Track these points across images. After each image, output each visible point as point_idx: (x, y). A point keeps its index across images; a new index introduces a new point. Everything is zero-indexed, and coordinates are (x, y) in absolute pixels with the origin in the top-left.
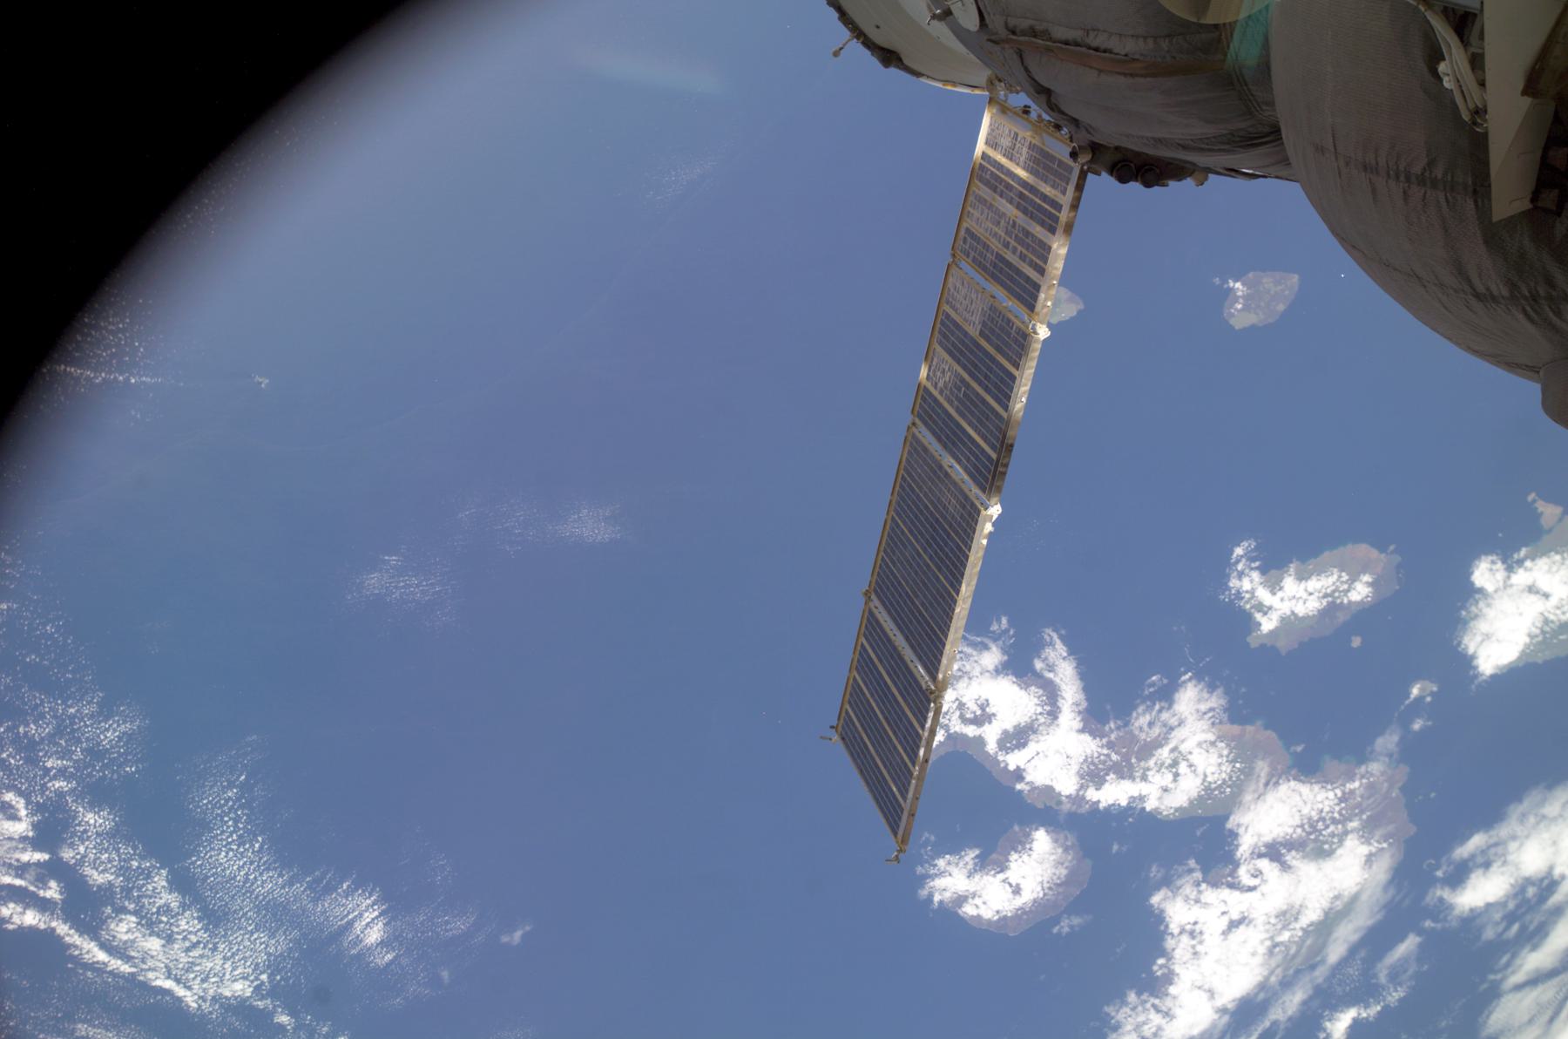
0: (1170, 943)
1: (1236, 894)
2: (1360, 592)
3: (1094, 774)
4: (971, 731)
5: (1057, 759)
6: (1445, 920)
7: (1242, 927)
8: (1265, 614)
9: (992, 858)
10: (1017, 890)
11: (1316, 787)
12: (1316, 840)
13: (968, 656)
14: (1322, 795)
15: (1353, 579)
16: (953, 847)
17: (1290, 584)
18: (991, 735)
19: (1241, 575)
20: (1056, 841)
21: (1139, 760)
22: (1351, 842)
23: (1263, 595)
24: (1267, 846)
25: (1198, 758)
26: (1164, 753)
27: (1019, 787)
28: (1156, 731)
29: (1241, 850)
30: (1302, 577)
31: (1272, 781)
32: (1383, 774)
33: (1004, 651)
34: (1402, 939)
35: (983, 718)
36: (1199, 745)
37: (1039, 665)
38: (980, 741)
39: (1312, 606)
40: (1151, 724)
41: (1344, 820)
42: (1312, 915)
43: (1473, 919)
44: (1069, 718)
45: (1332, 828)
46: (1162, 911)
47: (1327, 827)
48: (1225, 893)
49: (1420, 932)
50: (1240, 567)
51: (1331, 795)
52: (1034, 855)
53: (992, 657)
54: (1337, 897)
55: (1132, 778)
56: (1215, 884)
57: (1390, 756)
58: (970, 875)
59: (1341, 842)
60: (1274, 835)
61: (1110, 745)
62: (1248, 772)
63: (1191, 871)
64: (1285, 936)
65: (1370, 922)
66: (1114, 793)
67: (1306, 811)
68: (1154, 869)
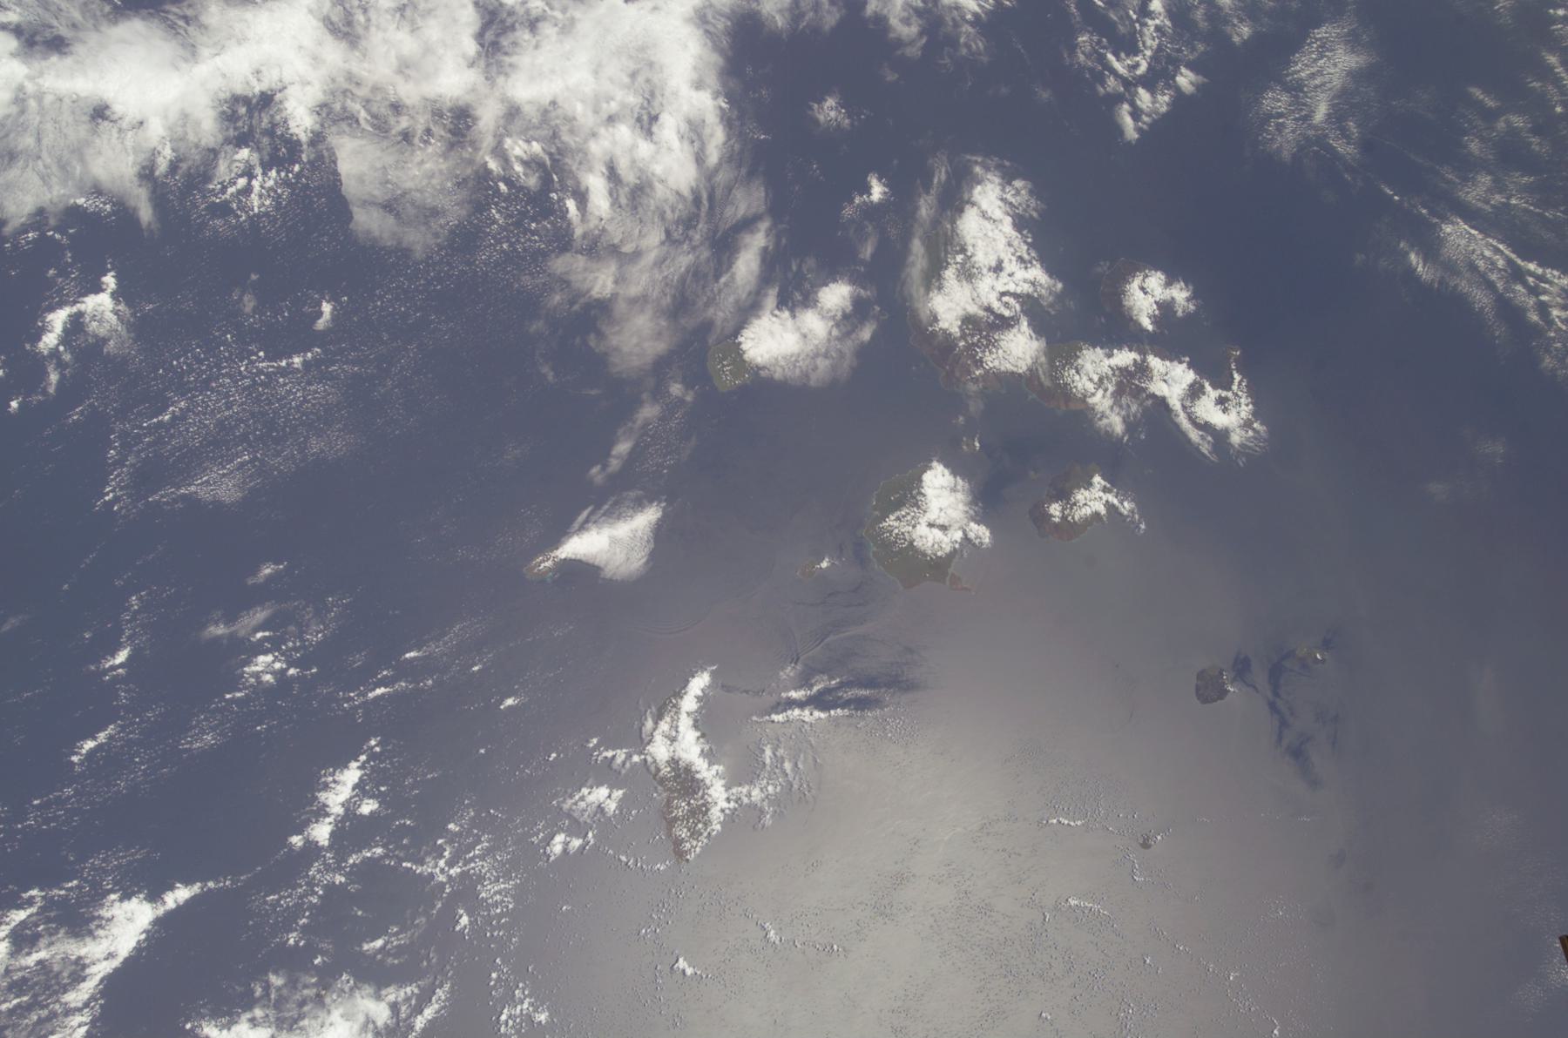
2: (1055, 509)
3: (1142, 370)
4: (1224, 394)
5: (1172, 380)
7: (993, 264)
9: (1166, 307)
10: (1142, 289)
12: (980, 331)
13: (1248, 439)
14: (996, 363)
15: (1064, 518)
16: (1189, 316)
17: (1103, 510)
18: (1212, 393)
19: (1132, 511)
22: (955, 330)
23: (1115, 502)
25: (1090, 387)
26: (1111, 389)
28: (1124, 401)
30: (1096, 515)
31: (1032, 371)
34: (873, 255)
35: (1221, 401)
38: (1215, 387)
39: (1081, 496)
41: (971, 347)
42: (950, 274)
43: (831, 274)
44: (1175, 403)
46: (1051, 276)
49: (863, 262)
53: (1236, 439)
54: (940, 288)
55: (1120, 369)
56: (1028, 296)
60: (1011, 336)
61: (1144, 390)
62: (1054, 379)
63: (1051, 305)
64: (959, 258)
66: (1124, 358)
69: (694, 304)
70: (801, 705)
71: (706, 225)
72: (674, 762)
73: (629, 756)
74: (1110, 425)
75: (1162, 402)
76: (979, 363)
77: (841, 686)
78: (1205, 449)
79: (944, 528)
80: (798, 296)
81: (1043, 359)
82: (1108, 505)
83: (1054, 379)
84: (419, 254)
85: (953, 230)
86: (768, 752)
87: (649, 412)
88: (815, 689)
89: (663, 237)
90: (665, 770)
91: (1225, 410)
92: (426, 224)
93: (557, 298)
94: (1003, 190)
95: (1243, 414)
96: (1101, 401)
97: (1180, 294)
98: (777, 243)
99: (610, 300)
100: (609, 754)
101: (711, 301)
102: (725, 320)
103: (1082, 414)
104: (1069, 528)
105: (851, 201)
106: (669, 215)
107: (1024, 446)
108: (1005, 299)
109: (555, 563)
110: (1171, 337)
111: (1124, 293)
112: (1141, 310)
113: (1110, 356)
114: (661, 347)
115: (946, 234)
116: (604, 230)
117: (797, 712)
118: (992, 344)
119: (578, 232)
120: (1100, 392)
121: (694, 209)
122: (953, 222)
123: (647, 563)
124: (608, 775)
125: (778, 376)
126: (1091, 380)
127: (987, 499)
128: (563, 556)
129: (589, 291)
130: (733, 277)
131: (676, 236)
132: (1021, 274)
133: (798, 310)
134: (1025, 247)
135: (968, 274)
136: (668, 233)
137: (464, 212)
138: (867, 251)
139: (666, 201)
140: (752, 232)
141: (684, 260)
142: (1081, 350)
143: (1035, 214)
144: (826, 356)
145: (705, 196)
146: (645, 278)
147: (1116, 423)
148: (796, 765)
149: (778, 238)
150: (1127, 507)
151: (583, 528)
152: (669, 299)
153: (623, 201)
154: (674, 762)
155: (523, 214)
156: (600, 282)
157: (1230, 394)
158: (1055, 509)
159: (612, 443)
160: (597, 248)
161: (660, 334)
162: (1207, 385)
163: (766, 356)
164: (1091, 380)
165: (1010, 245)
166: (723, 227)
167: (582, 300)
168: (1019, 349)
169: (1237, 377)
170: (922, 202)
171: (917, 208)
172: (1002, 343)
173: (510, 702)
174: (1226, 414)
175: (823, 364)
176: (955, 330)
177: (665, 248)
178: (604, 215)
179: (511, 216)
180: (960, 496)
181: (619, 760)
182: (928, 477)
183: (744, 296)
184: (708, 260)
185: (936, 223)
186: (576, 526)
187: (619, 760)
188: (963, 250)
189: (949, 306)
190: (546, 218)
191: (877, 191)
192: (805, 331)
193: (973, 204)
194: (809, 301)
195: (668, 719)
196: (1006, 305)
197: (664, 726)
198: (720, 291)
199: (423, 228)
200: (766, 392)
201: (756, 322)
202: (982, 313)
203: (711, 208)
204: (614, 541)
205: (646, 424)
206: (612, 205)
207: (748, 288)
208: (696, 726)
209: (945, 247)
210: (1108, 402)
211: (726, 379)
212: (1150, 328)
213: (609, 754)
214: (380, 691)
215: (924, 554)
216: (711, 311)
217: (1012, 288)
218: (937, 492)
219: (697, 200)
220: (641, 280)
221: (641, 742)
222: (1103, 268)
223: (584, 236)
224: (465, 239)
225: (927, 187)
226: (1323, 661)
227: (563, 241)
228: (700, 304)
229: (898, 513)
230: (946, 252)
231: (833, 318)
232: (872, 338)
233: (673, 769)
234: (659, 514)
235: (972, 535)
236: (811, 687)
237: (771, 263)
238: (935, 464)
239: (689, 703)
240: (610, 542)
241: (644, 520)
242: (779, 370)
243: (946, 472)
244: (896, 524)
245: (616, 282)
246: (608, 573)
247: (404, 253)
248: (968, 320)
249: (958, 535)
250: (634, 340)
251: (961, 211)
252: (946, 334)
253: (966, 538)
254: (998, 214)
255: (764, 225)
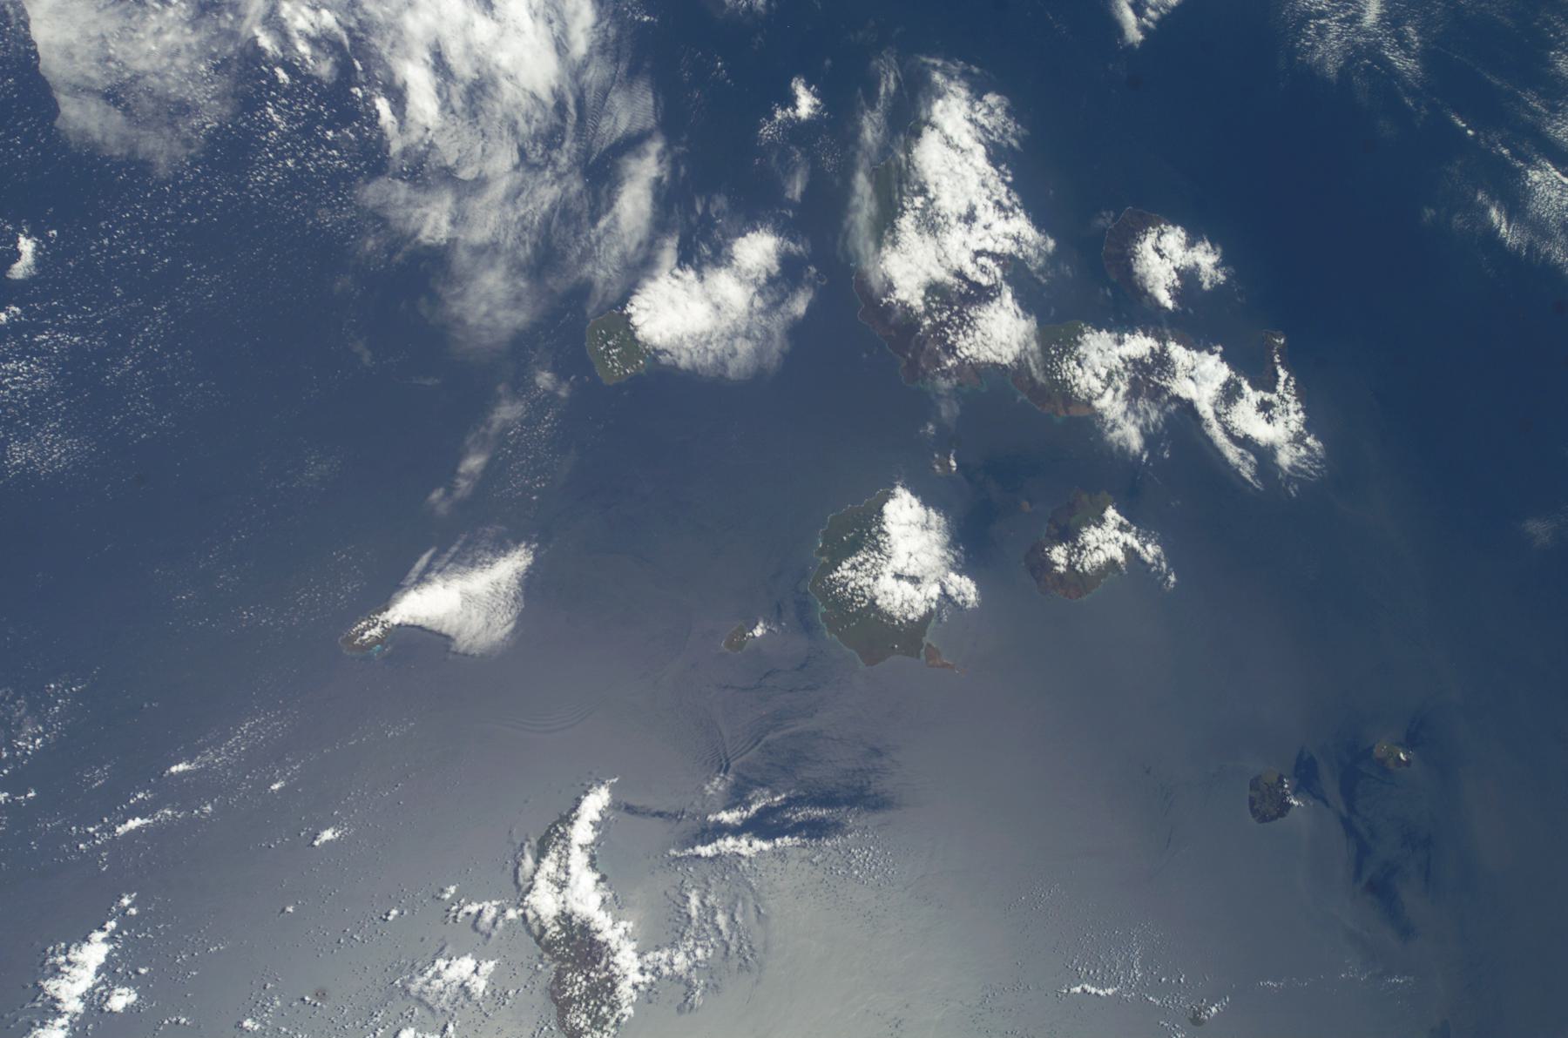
0: (1015, 199)
1: (990, 249)
2: (1059, 555)
3: (1162, 362)
4: (1267, 397)
5: (1201, 376)
6: (777, 221)
7: (964, 211)
8: (1121, 524)
9: (1188, 276)
10: (1158, 250)
11: (982, 358)
13: (1300, 459)
14: (973, 350)
15: (1071, 566)
16: (1217, 288)
18: (1252, 396)
19: (1157, 558)
20: (1156, 300)
21: (1136, 378)
22: (917, 302)
23: (1136, 544)
24: (992, 299)
25: (1097, 385)
26: (1124, 388)
27: (1220, 348)
28: (1142, 404)
29: (1009, 295)
30: (1112, 562)
32: (934, 378)
33: (1278, 466)
34: (803, 194)
35: (1264, 407)
36: (1101, 396)
37: (1252, 458)
39: (1091, 536)
40: (1147, 413)
41: (938, 326)
42: (906, 223)
43: (749, 221)
44: (1206, 409)
45: (945, 315)
46: (1039, 231)
47: (949, 318)
48: (998, 250)
49: (790, 204)
50: (1164, 565)
51: (967, 353)
52: (1162, 284)
53: (1285, 458)
54: (895, 243)
55: (1133, 361)
56: (1011, 257)
57: (939, 397)
58: (1197, 265)
59: (927, 303)
61: (1166, 389)
62: (1049, 373)
63: (1041, 271)
65: (852, 217)
66: (1139, 345)
67: (978, 334)
68: (1069, 273)
69: (564, 256)
70: (736, 831)
71: (576, 146)
72: (565, 918)
73: (502, 911)
74: (1124, 438)
75: (1188, 407)
76: (951, 350)
77: (789, 803)
78: (1247, 472)
79: (915, 580)
80: (706, 250)
81: (1034, 346)
82: (1128, 550)
83: (1049, 373)
84: (162, 169)
85: (908, 163)
86: (694, 901)
87: (507, 412)
88: (754, 808)
89: (516, 159)
90: (553, 930)
91: (1270, 420)
92: (172, 125)
93: (371, 243)
94: (972, 107)
95: (1293, 426)
96: (1111, 404)
97: (1205, 259)
98: (674, 173)
99: (446, 247)
100: (474, 908)
101: (587, 255)
102: (608, 281)
103: (1087, 422)
104: (1076, 580)
105: (771, 117)
106: (523, 127)
107: (1016, 463)
108: (982, 260)
109: (386, 631)
110: (1197, 316)
111: (1134, 255)
112: (1157, 280)
113: (1120, 342)
114: (520, 318)
115: (899, 167)
116: (431, 145)
117: (730, 841)
118: (966, 323)
119: (396, 146)
120: (1110, 393)
121: (559, 122)
122: (908, 151)
123: (514, 631)
124: (477, 938)
125: (684, 363)
126: (1097, 375)
127: (971, 543)
128: (396, 621)
129: (415, 233)
130: (615, 220)
131: (534, 157)
132: (1000, 226)
133: (708, 272)
134: (1004, 189)
135: (931, 224)
136: (522, 153)
137: (227, 111)
138: (796, 188)
139: (517, 106)
140: (638, 156)
141: (547, 194)
142: (1082, 333)
143: (1015, 143)
144: (747, 337)
145: (571, 101)
146: (493, 217)
147: (1130, 435)
148: (732, 918)
149: (675, 163)
150: (1151, 552)
151: (422, 580)
152: (529, 250)
153: (457, 103)
154: (565, 918)
155: (314, 117)
156: (431, 221)
157: (1274, 398)
158: (1059, 555)
159: (460, 457)
160: (424, 171)
161: (518, 299)
162: (1247, 388)
163: (667, 335)
164: (1097, 375)
165: (984, 185)
166: (600, 146)
167: (407, 248)
168: (1002, 332)
169: (1283, 374)
170: (865, 121)
171: (860, 129)
172: (979, 322)
173: (328, 835)
174: (1268, 425)
175: (744, 347)
176: (917, 302)
177: (519, 175)
178: (430, 124)
179: (296, 119)
180: (934, 535)
181: (488, 917)
182: (890, 508)
183: (632, 248)
184: (580, 194)
185: (885, 150)
186: (413, 575)
187: (488, 917)
188: (923, 191)
189: (909, 268)
190: (347, 124)
191: (806, 104)
192: (717, 299)
193: (934, 126)
194: (720, 257)
195: (554, 856)
196: (983, 269)
197: (549, 865)
198: (599, 239)
199: (167, 132)
200: (666, 383)
201: (650, 285)
202: (951, 280)
203: (581, 118)
204: (468, 598)
205: (506, 427)
206: (442, 108)
207: (637, 237)
208: (593, 864)
209: (897, 185)
210: (1120, 407)
211: (614, 366)
212: (1170, 304)
213: (474, 908)
214: (133, 824)
215: (891, 617)
216: (588, 268)
217: (989, 245)
218: (904, 529)
219: (560, 107)
220: (488, 221)
221: (521, 890)
222: (1105, 220)
223: (405, 153)
224: (231, 149)
225: (871, 98)
226: (1408, 763)
227: (372, 157)
228: (573, 258)
229: (853, 560)
230: (902, 193)
231: (755, 282)
232: (808, 310)
233: (564, 928)
234: (529, 560)
235: (952, 591)
236: (747, 806)
237: (667, 199)
238: (899, 490)
239: (582, 832)
240: (457, 601)
241: (509, 567)
242: (685, 355)
243: (915, 502)
244: (851, 574)
245: (453, 222)
246: (462, 644)
247: (139, 167)
248: (934, 289)
249: (934, 591)
250: (484, 308)
251: (918, 135)
252: (906, 308)
253: (945, 595)
254: (967, 141)
255: (655, 147)
